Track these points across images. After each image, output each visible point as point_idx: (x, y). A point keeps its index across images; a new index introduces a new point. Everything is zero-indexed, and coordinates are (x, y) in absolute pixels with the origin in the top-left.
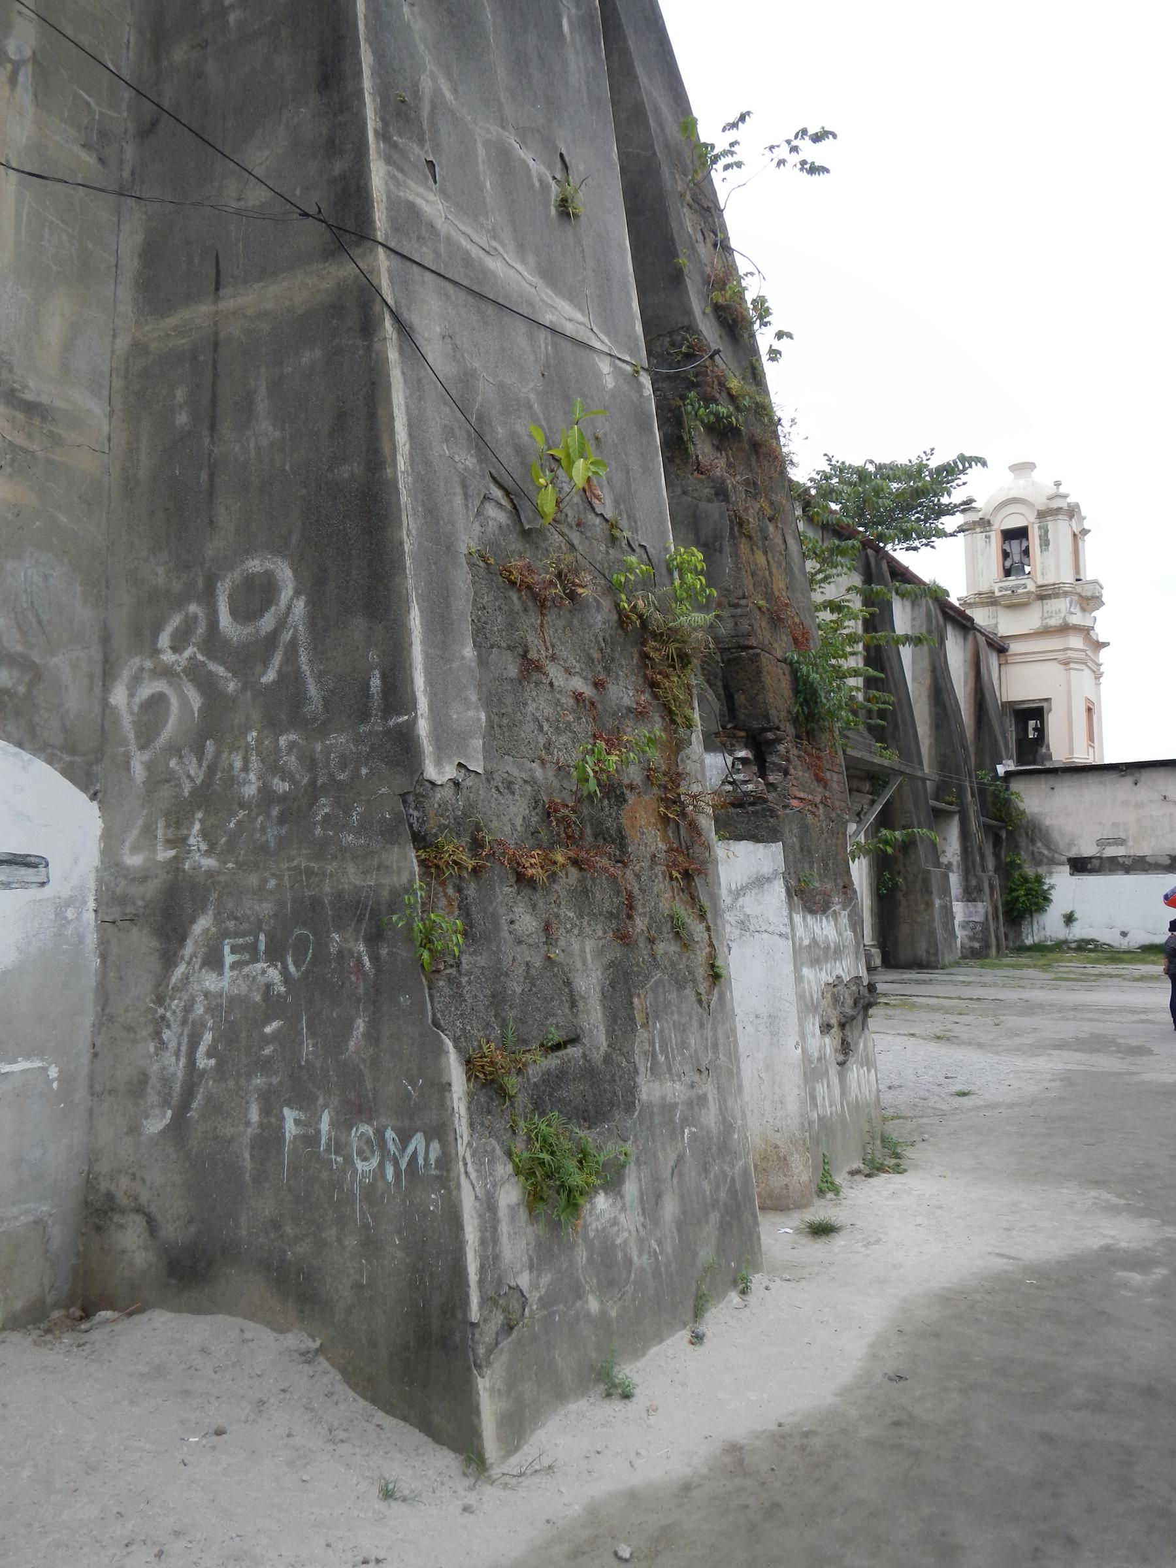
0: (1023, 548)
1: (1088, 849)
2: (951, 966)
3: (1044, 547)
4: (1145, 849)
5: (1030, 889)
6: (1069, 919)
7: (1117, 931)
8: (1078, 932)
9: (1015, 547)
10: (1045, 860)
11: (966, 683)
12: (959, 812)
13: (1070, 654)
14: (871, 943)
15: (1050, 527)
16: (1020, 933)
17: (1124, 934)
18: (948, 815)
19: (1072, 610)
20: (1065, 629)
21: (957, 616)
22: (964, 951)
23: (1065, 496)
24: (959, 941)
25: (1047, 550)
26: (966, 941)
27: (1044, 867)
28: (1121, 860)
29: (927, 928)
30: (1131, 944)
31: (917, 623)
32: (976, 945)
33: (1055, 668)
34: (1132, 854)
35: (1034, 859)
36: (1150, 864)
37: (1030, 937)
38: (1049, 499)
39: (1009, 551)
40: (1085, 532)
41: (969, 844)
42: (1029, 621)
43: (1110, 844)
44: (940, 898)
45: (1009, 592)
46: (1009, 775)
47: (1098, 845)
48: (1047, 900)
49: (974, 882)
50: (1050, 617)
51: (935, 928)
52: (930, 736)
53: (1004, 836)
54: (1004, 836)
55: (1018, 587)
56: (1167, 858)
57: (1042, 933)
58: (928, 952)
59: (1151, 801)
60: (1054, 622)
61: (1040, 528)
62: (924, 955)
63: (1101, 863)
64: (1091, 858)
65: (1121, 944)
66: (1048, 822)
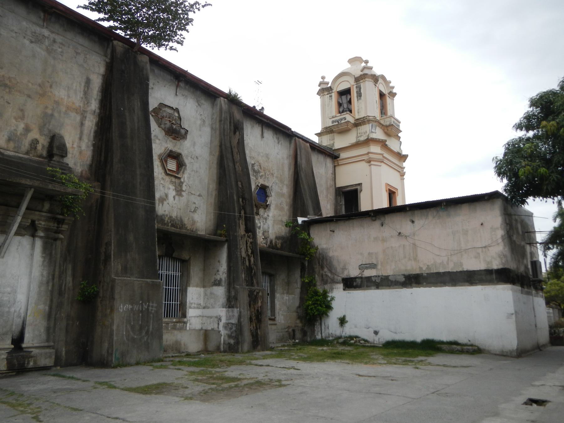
0: (348, 100)
1: (354, 272)
2: (138, 364)
3: (359, 98)
4: (389, 270)
5: (317, 300)
6: (343, 321)
7: (372, 331)
8: (349, 330)
9: (344, 99)
10: (329, 280)
11: (289, 169)
12: (227, 241)
13: (371, 155)
14: (42, 345)
15: (362, 86)
16: (313, 331)
17: (376, 333)
18: (221, 244)
19: (373, 130)
20: (368, 141)
21: (271, 123)
22: (225, 346)
23: (371, 68)
24: (222, 338)
25: (360, 99)
26: (226, 338)
27: (329, 285)
28: (373, 279)
30: (380, 340)
31: (215, 117)
32: (232, 341)
33: (364, 165)
34: (380, 274)
35: (323, 280)
36: (392, 282)
37: (319, 333)
38: (362, 71)
39: (341, 102)
40: (393, 95)
41: (232, 265)
42: (351, 138)
43: (367, 268)
45: (337, 123)
46: (307, 225)
47: (360, 269)
48: (329, 308)
49: (233, 294)
50: (361, 136)
51: (113, 330)
53: (307, 265)
54: (307, 265)
55: (341, 119)
56: (403, 276)
57: (327, 331)
58: (108, 352)
59: (392, 237)
60: (362, 138)
61: (357, 87)
63: (362, 281)
64: (355, 278)
65: (374, 340)
66: (331, 254)
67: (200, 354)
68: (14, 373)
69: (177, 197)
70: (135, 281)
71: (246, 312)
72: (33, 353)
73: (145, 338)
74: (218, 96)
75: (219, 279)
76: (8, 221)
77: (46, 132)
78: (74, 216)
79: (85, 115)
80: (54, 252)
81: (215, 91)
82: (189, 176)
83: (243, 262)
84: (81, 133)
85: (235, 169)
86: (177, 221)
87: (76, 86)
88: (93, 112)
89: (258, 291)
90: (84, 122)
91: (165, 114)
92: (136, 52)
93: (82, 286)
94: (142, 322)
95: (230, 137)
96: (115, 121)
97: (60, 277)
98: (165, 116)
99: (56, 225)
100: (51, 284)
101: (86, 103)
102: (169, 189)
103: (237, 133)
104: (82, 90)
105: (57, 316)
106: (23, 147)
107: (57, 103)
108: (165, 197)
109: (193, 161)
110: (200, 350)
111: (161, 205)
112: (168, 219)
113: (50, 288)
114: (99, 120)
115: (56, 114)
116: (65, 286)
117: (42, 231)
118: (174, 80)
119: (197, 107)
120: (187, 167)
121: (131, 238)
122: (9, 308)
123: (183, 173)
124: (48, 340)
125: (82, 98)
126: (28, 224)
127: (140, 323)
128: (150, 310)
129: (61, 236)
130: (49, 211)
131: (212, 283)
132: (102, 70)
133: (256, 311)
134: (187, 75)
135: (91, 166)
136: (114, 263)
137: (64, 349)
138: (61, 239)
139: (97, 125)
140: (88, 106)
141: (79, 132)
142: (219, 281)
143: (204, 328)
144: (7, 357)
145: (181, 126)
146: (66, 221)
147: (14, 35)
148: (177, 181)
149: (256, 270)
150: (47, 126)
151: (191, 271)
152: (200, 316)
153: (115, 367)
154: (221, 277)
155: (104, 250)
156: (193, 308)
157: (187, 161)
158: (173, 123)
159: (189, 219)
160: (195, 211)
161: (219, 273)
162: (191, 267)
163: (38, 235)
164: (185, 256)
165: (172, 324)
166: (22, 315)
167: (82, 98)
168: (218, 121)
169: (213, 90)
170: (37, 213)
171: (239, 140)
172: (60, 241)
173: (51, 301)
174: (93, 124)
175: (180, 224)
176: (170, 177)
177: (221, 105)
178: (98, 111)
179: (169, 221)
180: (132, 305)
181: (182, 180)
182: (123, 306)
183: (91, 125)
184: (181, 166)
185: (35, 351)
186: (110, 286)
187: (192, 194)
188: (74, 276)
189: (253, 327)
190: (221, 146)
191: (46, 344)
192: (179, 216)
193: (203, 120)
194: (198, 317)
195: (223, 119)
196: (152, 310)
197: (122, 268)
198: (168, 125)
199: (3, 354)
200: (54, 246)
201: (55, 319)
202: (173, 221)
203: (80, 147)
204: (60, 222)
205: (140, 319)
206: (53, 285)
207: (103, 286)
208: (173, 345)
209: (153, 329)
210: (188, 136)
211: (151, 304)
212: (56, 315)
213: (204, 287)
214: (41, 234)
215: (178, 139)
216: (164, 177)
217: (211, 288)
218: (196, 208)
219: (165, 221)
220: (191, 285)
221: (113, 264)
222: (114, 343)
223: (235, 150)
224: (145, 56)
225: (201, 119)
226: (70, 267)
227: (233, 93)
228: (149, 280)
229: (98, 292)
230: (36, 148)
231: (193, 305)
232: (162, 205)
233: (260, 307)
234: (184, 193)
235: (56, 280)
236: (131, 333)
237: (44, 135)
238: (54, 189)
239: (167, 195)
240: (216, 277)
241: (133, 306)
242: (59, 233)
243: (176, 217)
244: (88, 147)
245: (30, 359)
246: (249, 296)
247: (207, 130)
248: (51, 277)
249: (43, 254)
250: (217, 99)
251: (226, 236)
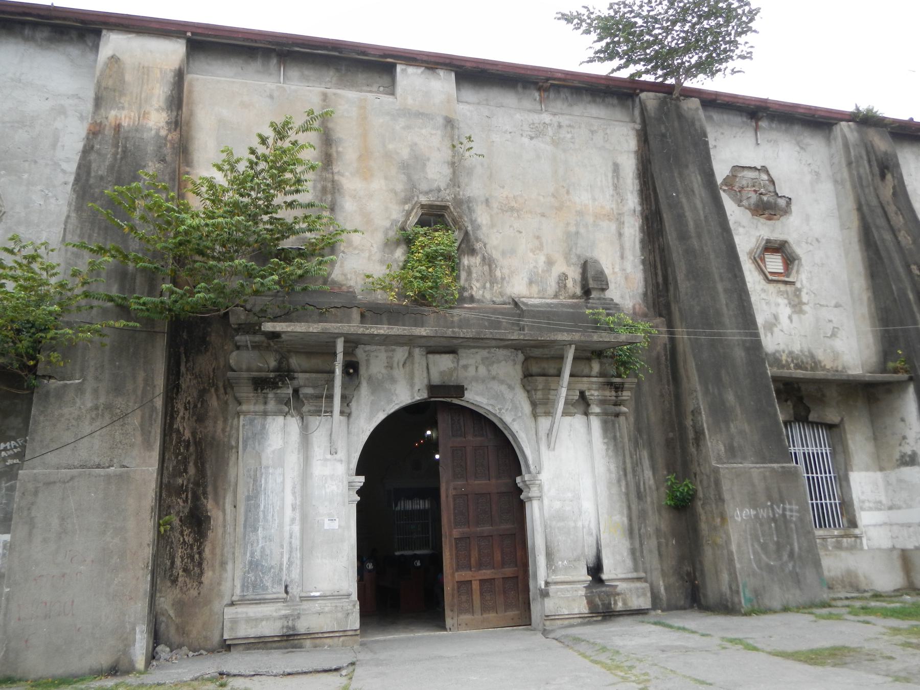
2: (786, 609)
14: (630, 576)
29: (725, 552)
52: (868, 289)
58: (731, 588)
62: (728, 592)
67: (902, 595)
68: (600, 618)
69: (795, 317)
70: (751, 468)
72: (618, 589)
73: (790, 565)
74: (835, 122)
75: (909, 453)
76: (551, 397)
77: (574, 259)
78: (636, 376)
79: (622, 220)
80: (618, 434)
81: (828, 114)
82: (809, 275)
84: (622, 248)
85: (899, 243)
86: (804, 358)
87: (601, 181)
88: (632, 212)
90: (622, 231)
91: (744, 182)
92: (678, 98)
93: (669, 483)
94: (778, 537)
95: (875, 189)
96: (666, 216)
97: (634, 471)
98: (745, 185)
99: (613, 393)
100: (623, 483)
101: (619, 201)
102: (778, 305)
103: (889, 177)
104: (610, 184)
105: (642, 531)
106: (549, 288)
107: (580, 213)
108: (774, 321)
109: (811, 248)
110: (898, 586)
111: (769, 335)
112: (788, 356)
113: (624, 490)
114: (643, 222)
115: (582, 231)
116: (644, 483)
117: (597, 405)
118: (749, 121)
119: (799, 153)
120: (803, 261)
121: (730, 397)
122: (575, 521)
123: (798, 272)
124: (636, 569)
125: (613, 196)
126: (577, 398)
127: (775, 539)
128: (788, 517)
129: (624, 409)
130: (602, 374)
131: (897, 460)
132: (632, 144)
134: (769, 105)
135: (645, 294)
136: (712, 442)
137: (661, 583)
138: (625, 414)
139: (642, 230)
140: (623, 206)
141: (618, 249)
142: (910, 456)
143: (898, 546)
144: (586, 593)
145: (777, 194)
146: (626, 386)
147: (508, 136)
148: (789, 288)
150: (574, 250)
151: (850, 442)
152: (885, 524)
153: (745, 614)
154: (915, 449)
155: (691, 423)
156: (868, 510)
157: (800, 250)
158: (761, 194)
159: (825, 350)
160: (834, 335)
161: (907, 441)
162: (849, 436)
163: (593, 411)
164: (832, 416)
165: (834, 540)
166: (594, 532)
167: (613, 196)
168: (844, 165)
169: (823, 114)
170: (585, 379)
171: (894, 188)
172: (624, 418)
173: (629, 508)
174: (635, 231)
175: (810, 362)
176: (775, 285)
177: (844, 137)
178: (639, 208)
179: (789, 360)
180: (755, 508)
181: (798, 285)
182: (741, 511)
183: (633, 233)
184: (791, 262)
185: (622, 586)
186: (712, 479)
187: (821, 305)
188: (654, 468)
190: (860, 209)
191: (635, 575)
192: (806, 349)
193: (816, 172)
194: (881, 525)
195: (853, 159)
196: (791, 516)
197: (725, 449)
198: (754, 198)
199: (579, 589)
200: (617, 425)
201: (640, 536)
202: (797, 359)
203: (624, 270)
204: (618, 388)
205: (774, 532)
206: (627, 484)
207: (701, 481)
208: (843, 577)
209: (800, 548)
210: (794, 207)
211: (788, 506)
212: (639, 530)
213: (881, 469)
214: (595, 409)
215: (775, 217)
216: (765, 288)
217: (897, 470)
218: (836, 330)
219: (781, 361)
220: (854, 468)
221: (709, 444)
222: (738, 574)
223: (891, 209)
224: (693, 99)
225: (811, 172)
226: (645, 454)
227: (863, 107)
228: (775, 465)
229: (695, 491)
230: (565, 286)
231: (867, 505)
232: (772, 334)
234: (805, 308)
235: (630, 476)
236: (764, 557)
237: (573, 264)
238: (601, 339)
239: (776, 317)
240: (902, 448)
241: (757, 510)
242: (620, 405)
243: (801, 351)
244: (635, 266)
245: (617, 598)
247: (827, 189)
248: (621, 473)
249: (604, 439)
250: (834, 127)
251: (906, 371)
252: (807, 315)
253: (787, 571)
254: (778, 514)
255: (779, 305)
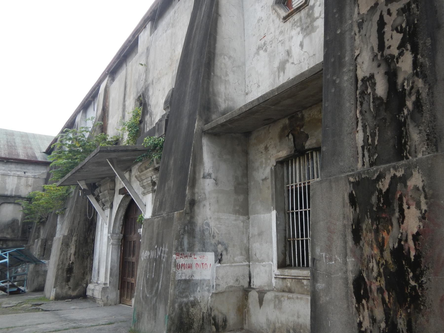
44: (150, 249)
69: (306, 42)
71: (340, 260)
83: (363, 93)
89: (399, 174)
102: (291, 38)
108: (287, 58)
111: (282, 74)
133: (387, 255)
149: (424, 95)
189: (373, 320)
232: (284, 73)
233: (416, 237)
239: (289, 53)
246: (353, 201)
252: (318, 30)
253: (153, 303)
254: (158, 255)
255: (292, 37)
